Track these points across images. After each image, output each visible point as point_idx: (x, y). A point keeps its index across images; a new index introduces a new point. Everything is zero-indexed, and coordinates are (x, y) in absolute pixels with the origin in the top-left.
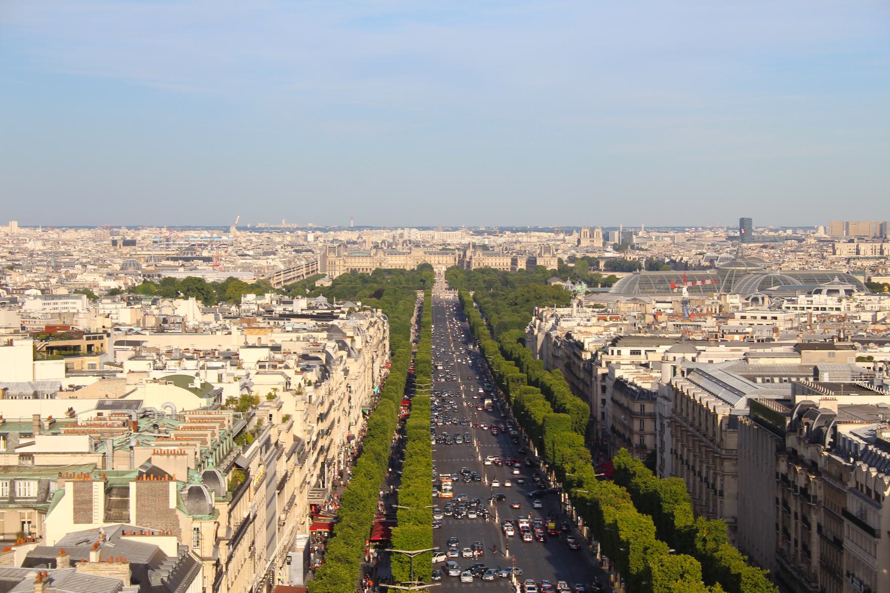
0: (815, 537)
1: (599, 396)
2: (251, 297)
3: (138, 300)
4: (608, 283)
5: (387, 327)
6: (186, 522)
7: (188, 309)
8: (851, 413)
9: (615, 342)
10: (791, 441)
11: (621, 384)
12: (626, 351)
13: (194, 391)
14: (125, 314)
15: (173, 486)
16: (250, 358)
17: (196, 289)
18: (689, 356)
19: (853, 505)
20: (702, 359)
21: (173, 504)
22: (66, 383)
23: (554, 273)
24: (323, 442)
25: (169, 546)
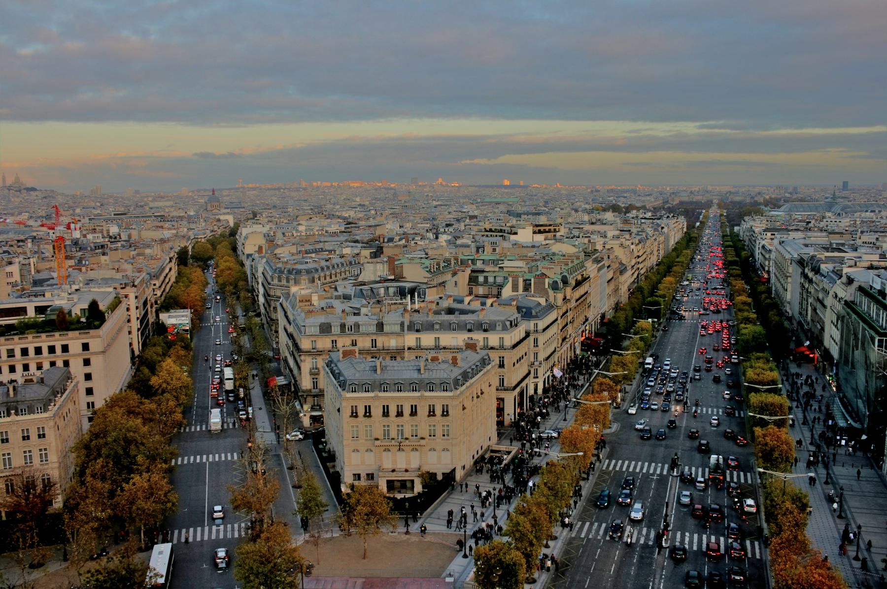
0: (810, 308)
1: (757, 251)
2: (634, 212)
3: (593, 212)
4: (779, 207)
5: (685, 224)
6: (551, 292)
7: (609, 216)
8: (828, 260)
9: (765, 231)
10: (806, 270)
11: (763, 247)
12: (769, 234)
13: (574, 246)
14: (586, 218)
15: (547, 280)
16: (610, 234)
17: (615, 208)
18: (785, 236)
19: (821, 296)
20: (790, 238)
21: (547, 286)
22: (544, 243)
23: (760, 204)
24: (640, 266)
25: (542, 301)
